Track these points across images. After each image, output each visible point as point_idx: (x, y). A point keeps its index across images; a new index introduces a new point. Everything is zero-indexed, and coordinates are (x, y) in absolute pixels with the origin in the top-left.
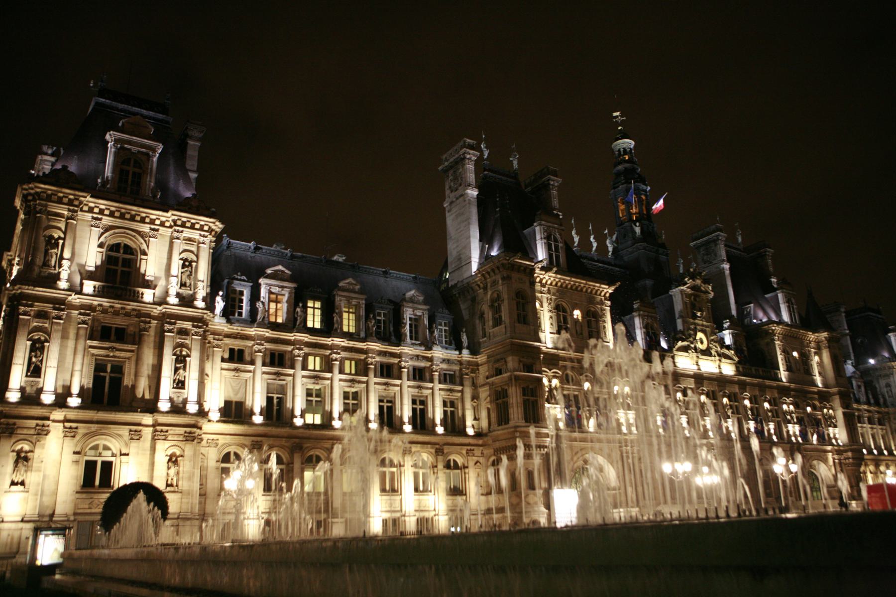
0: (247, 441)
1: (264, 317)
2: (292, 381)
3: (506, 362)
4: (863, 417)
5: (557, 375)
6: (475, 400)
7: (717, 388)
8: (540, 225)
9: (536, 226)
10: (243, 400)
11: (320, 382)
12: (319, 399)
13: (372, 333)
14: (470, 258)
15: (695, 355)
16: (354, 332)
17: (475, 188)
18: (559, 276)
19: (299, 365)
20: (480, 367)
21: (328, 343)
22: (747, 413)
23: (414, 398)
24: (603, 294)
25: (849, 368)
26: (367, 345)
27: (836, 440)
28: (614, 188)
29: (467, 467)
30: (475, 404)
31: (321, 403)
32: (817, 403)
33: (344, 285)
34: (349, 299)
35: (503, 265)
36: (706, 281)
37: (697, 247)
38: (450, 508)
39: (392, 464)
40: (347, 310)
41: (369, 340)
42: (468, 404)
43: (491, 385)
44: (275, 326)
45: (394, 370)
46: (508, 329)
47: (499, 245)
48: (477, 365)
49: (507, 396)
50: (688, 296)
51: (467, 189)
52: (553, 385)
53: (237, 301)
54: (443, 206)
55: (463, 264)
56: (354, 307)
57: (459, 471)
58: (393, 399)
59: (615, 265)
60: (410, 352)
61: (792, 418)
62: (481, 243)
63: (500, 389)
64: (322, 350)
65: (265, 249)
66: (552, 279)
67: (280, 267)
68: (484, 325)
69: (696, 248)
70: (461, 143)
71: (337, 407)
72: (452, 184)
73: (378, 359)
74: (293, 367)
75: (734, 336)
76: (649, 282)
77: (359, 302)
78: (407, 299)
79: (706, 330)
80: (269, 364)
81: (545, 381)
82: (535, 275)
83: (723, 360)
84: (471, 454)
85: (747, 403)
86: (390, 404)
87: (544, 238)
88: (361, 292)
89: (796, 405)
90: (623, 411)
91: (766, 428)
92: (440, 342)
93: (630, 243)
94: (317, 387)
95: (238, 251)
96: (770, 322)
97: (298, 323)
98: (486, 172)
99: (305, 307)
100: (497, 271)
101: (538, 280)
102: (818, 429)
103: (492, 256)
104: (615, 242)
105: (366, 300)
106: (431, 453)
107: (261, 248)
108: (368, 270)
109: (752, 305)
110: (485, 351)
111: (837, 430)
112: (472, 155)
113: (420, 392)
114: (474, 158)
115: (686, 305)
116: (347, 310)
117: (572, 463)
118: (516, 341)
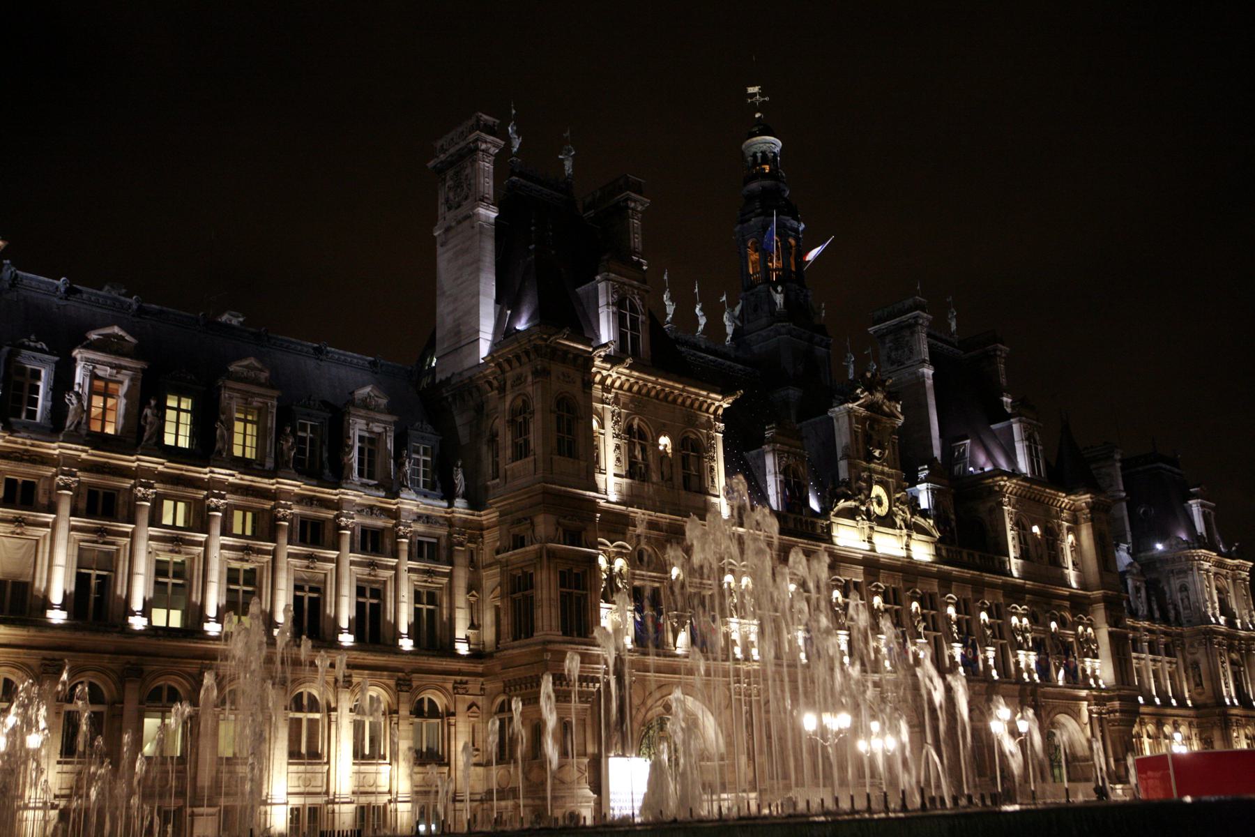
0: (33, 658)
1: (79, 423)
2: (128, 547)
3: (532, 524)
4: (1142, 641)
5: (624, 551)
6: (474, 592)
7: (901, 585)
8: (607, 279)
9: (599, 282)
10: (29, 580)
11: (184, 549)
12: (180, 582)
13: (288, 462)
14: (478, 331)
15: (866, 524)
16: (254, 457)
17: (492, 204)
18: (636, 374)
19: (143, 517)
20: (484, 532)
21: (202, 476)
22: (950, 629)
23: (361, 584)
24: (712, 410)
25: (1123, 557)
26: (278, 483)
27: (1096, 679)
28: (742, 222)
29: (454, 714)
30: (472, 599)
31: (184, 589)
32: (1068, 615)
33: (238, 368)
34: (247, 397)
35: (537, 349)
36: (892, 396)
37: (881, 336)
38: (415, 789)
39: (314, 705)
40: (242, 416)
41: (281, 475)
42: (461, 599)
43: (504, 565)
44: (100, 441)
45: (326, 531)
46: (540, 465)
47: (530, 312)
48: (481, 528)
49: (532, 587)
50: (861, 420)
51: (479, 206)
52: (616, 568)
53: (27, 390)
54: (432, 232)
55: (463, 343)
56: (256, 413)
57: (439, 720)
58: (321, 586)
59: (736, 360)
60: (358, 500)
61: (1025, 639)
62: (499, 306)
63: (520, 573)
64: (190, 490)
65: (87, 293)
66: (623, 378)
67: (116, 330)
68: (497, 456)
69: (878, 337)
70: (473, 121)
71: (214, 599)
72: (451, 195)
73: (296, 510)
74: (131, 519)
75: (935, 494)
76: (793, 393)
77: (267, 404)
78: (356, 401)
79: (887, 482)
80: (84, 512)
81: (602, 561)
82: (594, 370)
83: (915, 535)
84: (461, 691)
85: (951, 611)
86: (315, 595)
87: (613, 304)
88: (271, 385)
89: (1033, 618)
90: (737, 620)
91: (981, 656)
92: (415, 483)
93: (764, 321)
94: (178, 558)
95: (33, 294)
96: (997, 472)
97: (146, 435)
98: (514, 178)
99: (162, 408)
100: (524, 359)
101: (598, 378)
102: (1067, 660)
103: (518, 331)
104: (738, 318)
105: (279, 399)
106: (388, 686)
107: (80, 292)
108: (286, 344)
109: (968, 441)
110: (496, 503)
111: (1097, 663)
112: (491, 144)
113: (373, 573)
114: (494, 150)
115: (857, 437)
116: (242, 416)
117: (643, 711)
118: (554, 486)
